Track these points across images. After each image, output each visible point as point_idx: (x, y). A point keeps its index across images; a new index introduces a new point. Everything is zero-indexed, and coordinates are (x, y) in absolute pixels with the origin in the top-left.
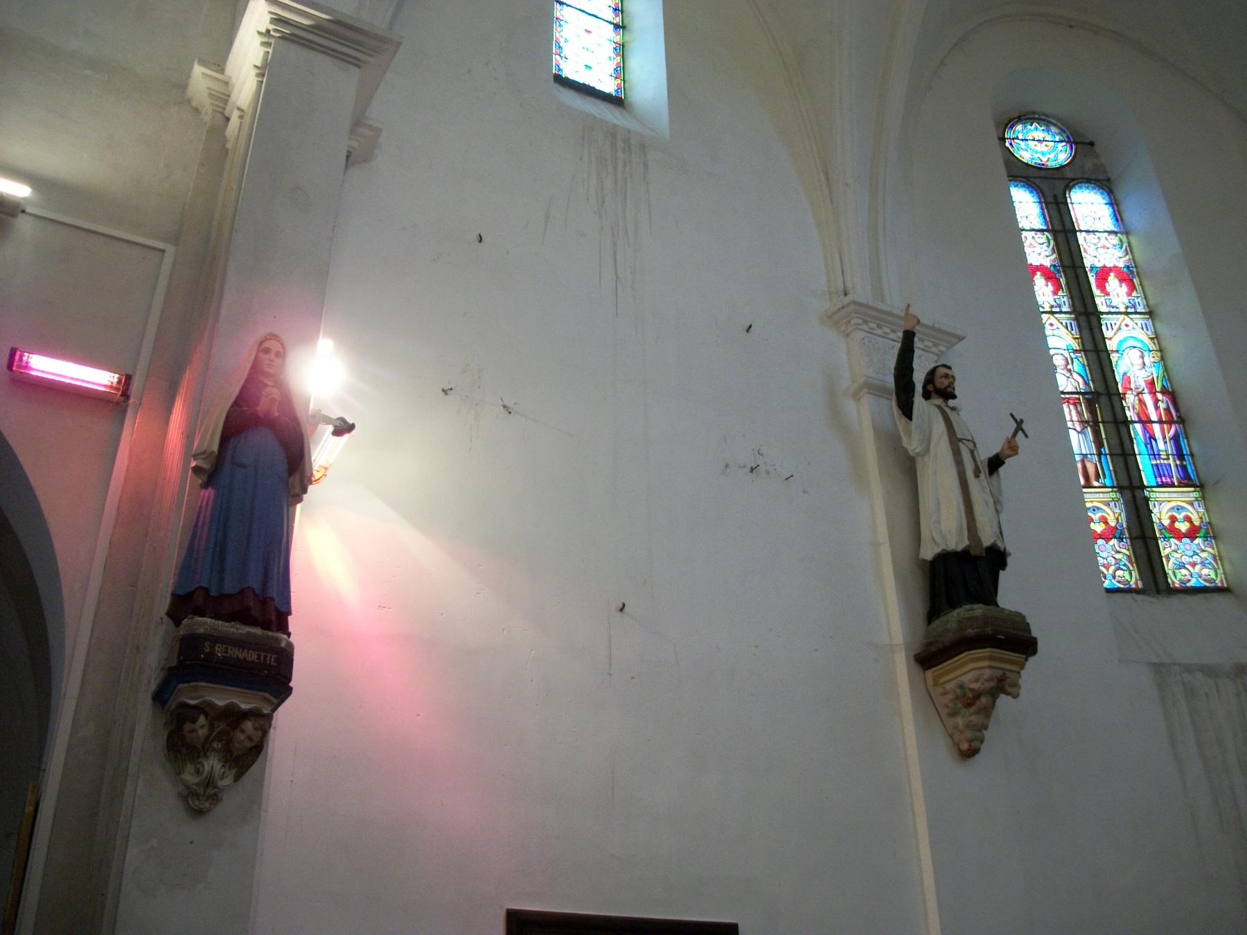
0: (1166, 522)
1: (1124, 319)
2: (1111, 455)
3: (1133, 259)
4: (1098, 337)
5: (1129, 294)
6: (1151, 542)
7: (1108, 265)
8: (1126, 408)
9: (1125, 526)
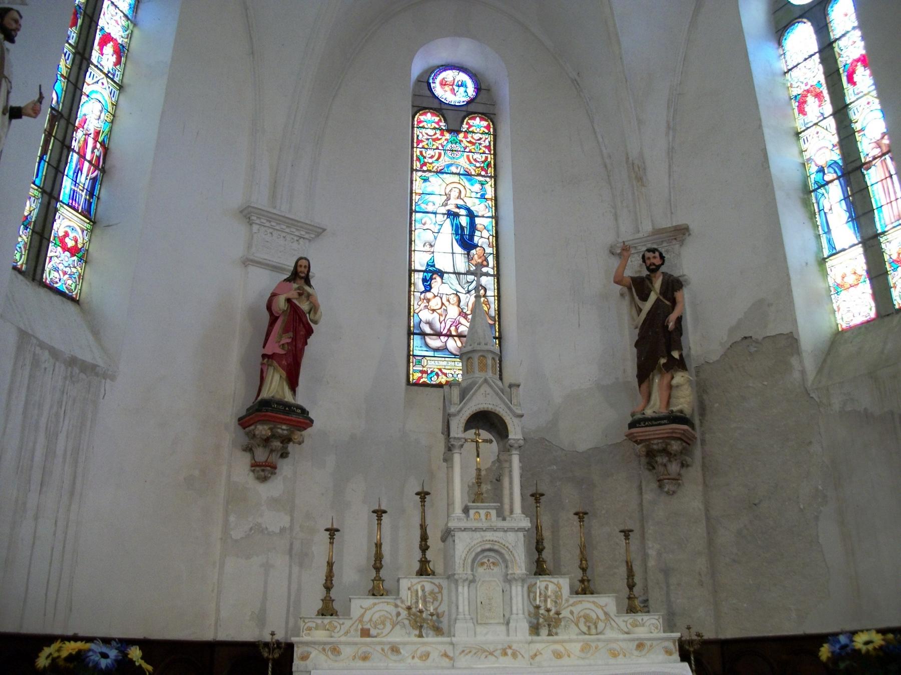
0: (61, 234)
1: (103, 78)
2: (49, 164)
3: (129, 44)
4: (81, 76)
5: (115, 65)
6: (45, 242)
7: (112, 35)
8: (74, 139)
9: (33, 220)
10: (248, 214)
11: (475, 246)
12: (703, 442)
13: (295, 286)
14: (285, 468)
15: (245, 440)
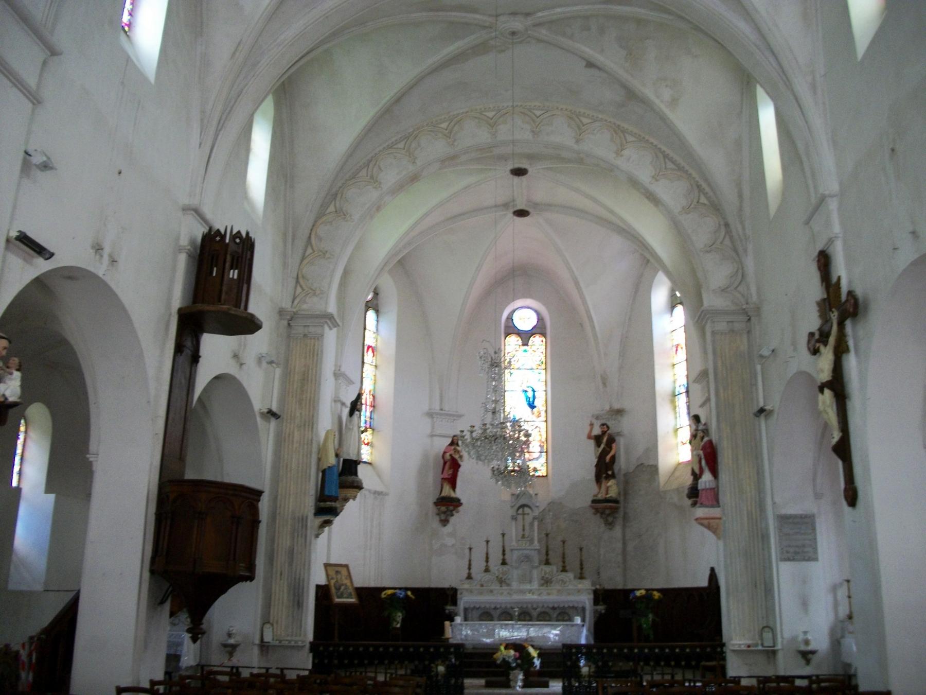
10: (430, 415)
11: (535, 407)
13: (453, 447)
14: (452, 520)
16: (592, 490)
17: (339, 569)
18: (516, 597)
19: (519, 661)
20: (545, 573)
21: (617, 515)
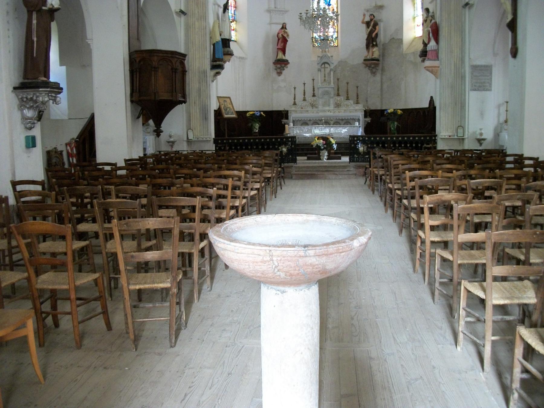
10: (269, 11)
11: (330, 5)
12: (382, 63)
13: (283, 30)
14: (284, 72)
15: (275, 67)
16: (364, 54)
17: (226, 99)
18: (321, 114)
19: (325, 146)
20: (337, 101)
21: (377, 68)
